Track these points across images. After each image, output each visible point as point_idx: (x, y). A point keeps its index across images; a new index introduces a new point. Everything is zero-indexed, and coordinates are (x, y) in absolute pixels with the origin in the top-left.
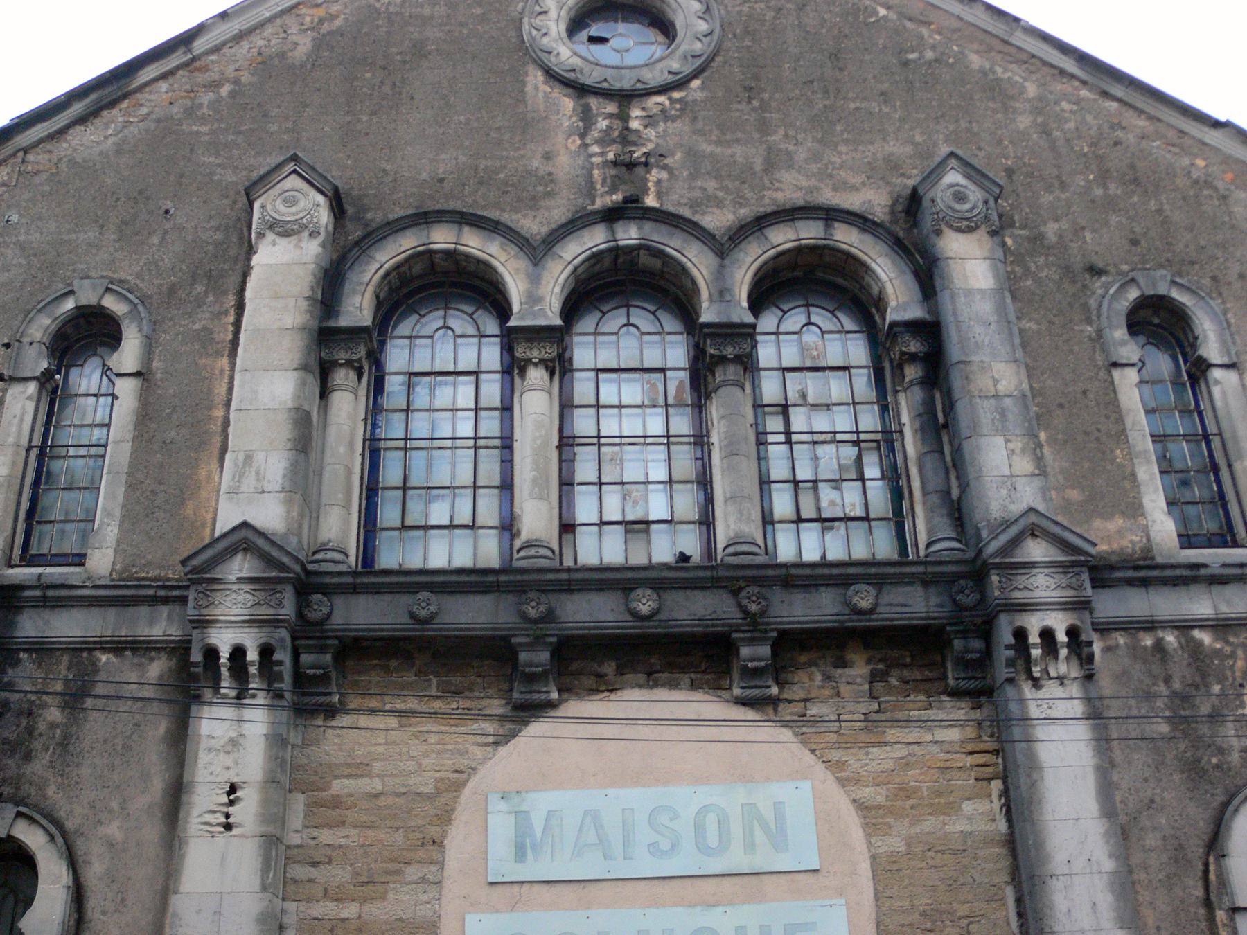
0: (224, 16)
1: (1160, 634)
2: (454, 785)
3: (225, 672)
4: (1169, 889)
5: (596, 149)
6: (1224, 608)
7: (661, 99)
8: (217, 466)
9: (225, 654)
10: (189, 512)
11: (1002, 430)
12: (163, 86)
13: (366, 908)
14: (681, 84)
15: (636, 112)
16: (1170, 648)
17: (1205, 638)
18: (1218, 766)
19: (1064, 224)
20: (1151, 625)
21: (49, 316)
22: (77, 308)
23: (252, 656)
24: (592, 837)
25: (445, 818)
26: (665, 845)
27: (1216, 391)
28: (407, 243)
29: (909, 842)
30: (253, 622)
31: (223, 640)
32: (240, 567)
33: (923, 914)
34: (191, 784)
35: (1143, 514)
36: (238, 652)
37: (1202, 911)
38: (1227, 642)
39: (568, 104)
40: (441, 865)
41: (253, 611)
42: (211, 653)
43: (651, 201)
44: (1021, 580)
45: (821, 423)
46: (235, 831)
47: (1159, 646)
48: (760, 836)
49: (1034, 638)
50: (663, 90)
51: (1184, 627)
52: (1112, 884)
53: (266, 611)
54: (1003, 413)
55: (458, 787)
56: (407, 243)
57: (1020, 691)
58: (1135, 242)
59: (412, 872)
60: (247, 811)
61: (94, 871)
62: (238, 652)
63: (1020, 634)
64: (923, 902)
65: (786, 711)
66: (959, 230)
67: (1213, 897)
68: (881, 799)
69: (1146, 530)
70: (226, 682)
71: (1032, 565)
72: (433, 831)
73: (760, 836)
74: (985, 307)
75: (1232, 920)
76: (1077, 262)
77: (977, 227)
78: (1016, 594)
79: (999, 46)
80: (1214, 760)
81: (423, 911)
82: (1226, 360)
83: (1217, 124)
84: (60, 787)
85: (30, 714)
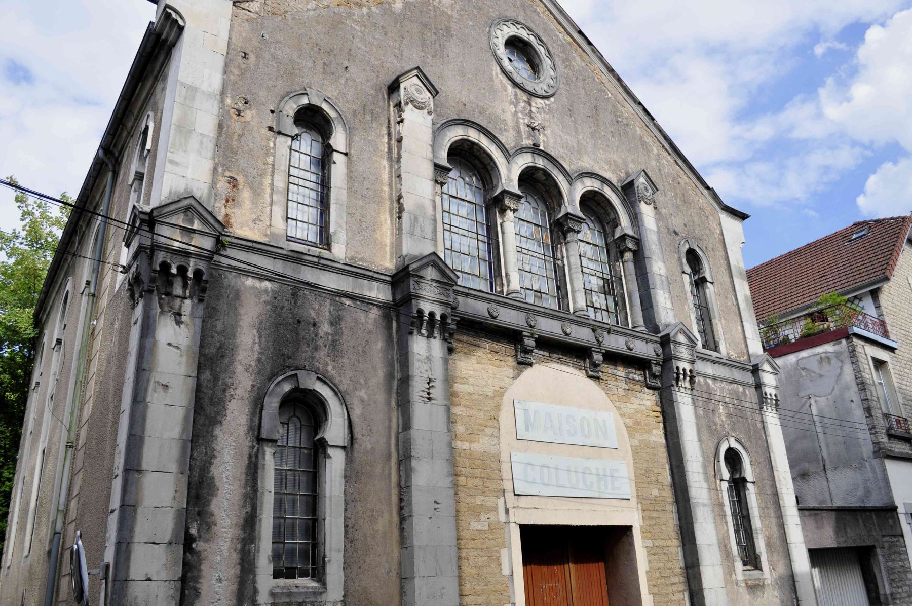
3: (425, 324)
5: (520, 115)
9: (426, 313)
10: (378, 236)
11: (663, 289)
13: (472, 445)
21: (295, 103)
22: (309, 104)
23: (438, 317)
27: (707, 291)
29: (640, 441)
30: (441, 303)
31: (427, 307)
34: (412, 376)
36: (432, 314)
41: (438, 296)
42: (420, 312)
43: (541, 148)
46: (433, 402)
53: (443, 298)
55: (501, 395)
58: (685, 225)
61: (356, 413)
62: (432, 314)
81: (493, 449)
83: (708, 188)
84: (334, 368)
85: (314, 325)
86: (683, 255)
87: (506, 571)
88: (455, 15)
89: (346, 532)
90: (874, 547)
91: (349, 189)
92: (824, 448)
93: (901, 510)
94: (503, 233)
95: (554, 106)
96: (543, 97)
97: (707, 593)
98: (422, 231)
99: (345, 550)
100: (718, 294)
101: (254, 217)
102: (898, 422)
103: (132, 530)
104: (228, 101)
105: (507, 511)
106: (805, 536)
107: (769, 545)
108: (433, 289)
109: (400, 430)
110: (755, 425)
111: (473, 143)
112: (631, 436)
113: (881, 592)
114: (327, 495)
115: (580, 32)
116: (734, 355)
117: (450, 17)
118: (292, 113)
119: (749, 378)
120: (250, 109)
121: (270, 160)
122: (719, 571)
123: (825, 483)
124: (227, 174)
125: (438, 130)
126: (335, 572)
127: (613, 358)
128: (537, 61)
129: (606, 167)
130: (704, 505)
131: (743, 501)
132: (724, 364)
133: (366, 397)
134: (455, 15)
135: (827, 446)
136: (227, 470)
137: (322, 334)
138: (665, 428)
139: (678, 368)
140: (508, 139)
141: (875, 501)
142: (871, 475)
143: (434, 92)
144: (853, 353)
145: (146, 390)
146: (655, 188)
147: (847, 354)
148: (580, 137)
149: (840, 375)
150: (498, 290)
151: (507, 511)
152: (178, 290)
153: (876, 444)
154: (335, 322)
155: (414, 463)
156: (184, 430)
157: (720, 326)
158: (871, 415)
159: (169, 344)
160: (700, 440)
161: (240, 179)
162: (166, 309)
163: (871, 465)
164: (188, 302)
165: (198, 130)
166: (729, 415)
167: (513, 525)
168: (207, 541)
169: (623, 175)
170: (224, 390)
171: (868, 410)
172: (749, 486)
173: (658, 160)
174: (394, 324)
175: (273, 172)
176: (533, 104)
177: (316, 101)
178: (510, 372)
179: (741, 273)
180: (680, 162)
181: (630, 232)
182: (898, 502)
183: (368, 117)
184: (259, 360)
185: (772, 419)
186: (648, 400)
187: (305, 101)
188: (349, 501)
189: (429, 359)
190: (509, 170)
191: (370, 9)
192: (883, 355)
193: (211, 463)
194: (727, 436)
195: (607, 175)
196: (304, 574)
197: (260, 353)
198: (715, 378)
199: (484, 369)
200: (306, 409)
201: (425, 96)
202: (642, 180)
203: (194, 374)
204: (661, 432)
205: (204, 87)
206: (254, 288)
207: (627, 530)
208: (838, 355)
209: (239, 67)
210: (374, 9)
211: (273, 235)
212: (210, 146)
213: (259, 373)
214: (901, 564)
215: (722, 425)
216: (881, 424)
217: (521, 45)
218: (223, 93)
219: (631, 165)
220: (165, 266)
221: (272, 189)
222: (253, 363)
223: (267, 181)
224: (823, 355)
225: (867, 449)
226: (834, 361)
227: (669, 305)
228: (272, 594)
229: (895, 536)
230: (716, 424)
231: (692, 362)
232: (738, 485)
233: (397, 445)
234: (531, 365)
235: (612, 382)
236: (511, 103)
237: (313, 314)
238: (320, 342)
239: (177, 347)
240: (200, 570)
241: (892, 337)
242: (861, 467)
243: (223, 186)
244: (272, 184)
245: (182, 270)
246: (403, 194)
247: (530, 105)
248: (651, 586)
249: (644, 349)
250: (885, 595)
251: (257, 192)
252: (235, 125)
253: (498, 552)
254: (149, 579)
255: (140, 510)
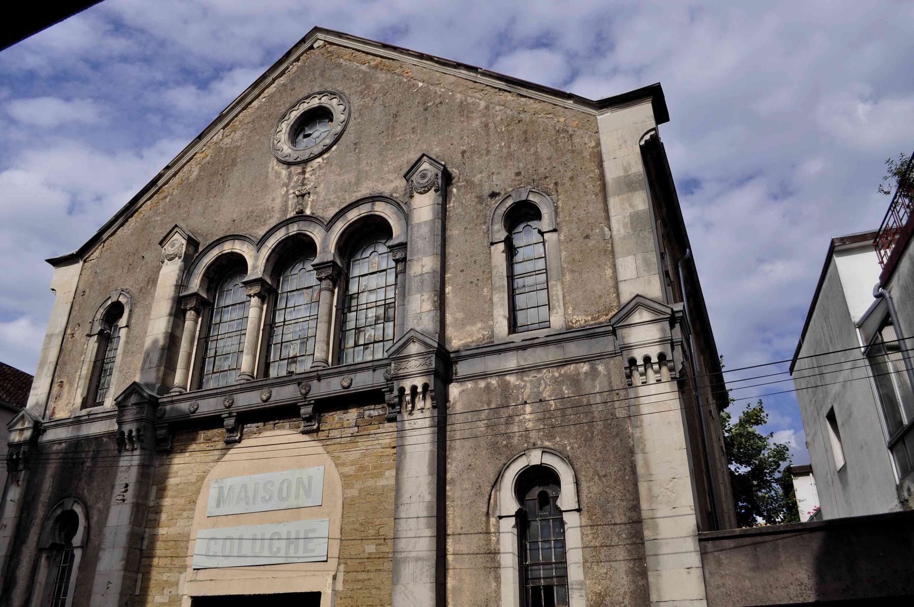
0: (168, 168)
1: (489, 380)
2: (201, 479)
4: (470, 508)
6: (522, 363)
7: (320, 160)
12: (149, 202)
14: (328, 149)
15: (309, 169)
16: (492, 387)
17: (512, 379)
18: (506, 446)
19: (484, 174)
20: (484, 376)
24: (243, 495)
25: (198, 492)
26: (267, 497)
28: (215, 253)
29: (360, 491)
30: (136, 420)
33: (361, 524)
35: (492, 320)
37: (484, 519)
38: (522, 380)
40: (194, 510)
43: (308, 212)
44: (404, 365)
45: (373, 298)
47: (488, 387)
48: (302, 492)
49: (408, 391)
50: (320, 155)
51: (501, 374)
52: (428, 507)
54: (422, 283)
56: (215, 253)
57: (403, 417)
59: (185, 514)
63: (402, 390)
64: (361, 518)
65: (322, 435)
66: (421, 193)
67: (490, 512)
68: (352, 473)
69: (492, 328)
71: (409, 356)
72: (194, 497)
73: (302, 492)
74: (425, 230)
75: (498, 522)
76: (487, 191)
77: (429, 190)
78: (401, 371)
79: (470, 84)
80: (504, 442)
82: (551, 228)
115: (385, 46)
167: (185, 597)
180: (524, 91)
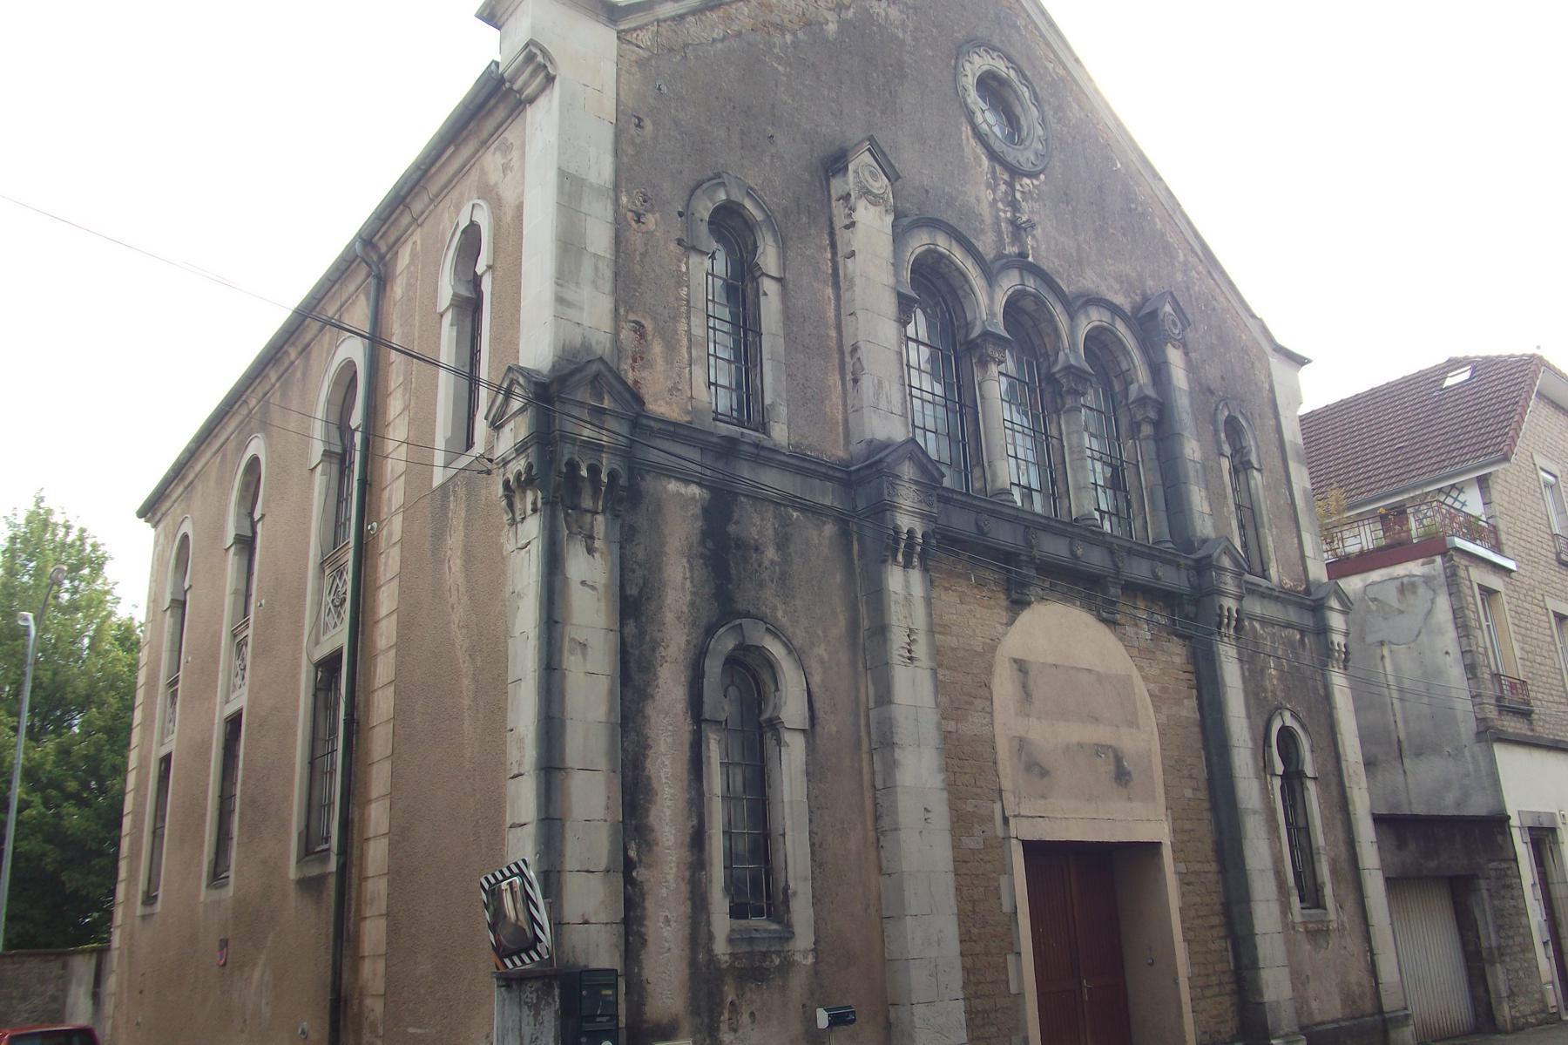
5: (1000, 205)
8: (837, 377)
21: (711, 200)
27: (1252, 483)
32: (907, 471)
36: (910, 532)
39: (985, 161)
42: (897, 531)
55: (993, 649)
60: (921, 650)
61: (816, 679)
62: (910, 532)
70: (900, 558)
83: (1253, 316)
84: (785, 613)
85: (757, 549)
86: (1221, 427)
87: (1007, 908)
88: (909, 40)
89: (813, 853)
90: (1476, 877)
91: (787, 335)
92: (1400, 724)
93: (1514, 821)
94: (982, 397)
95: (1044, 188)
96: (1030, 175)
97: (1259, 940)
98: (889, 402)
99: (813, 879)
100: (1267, 487)
101: (670, 384)
102: (1513, 686)
103: (561, 854)
104: (624, 199)
105: (1006, 820)
106: (1382, 860)
107: (1333, 871)
108: (911, 494)
109: (872, 705)
110: (1316, 690)
111: (941, 255)
112: (1157, 710)
113: (1484, 944)
114: (786, 799)
116: (1288, 584)
117: (903, 43)
118: (706, 216)
119: (1308, 620)
120: (652, 211)
121: (684, 292)
122: (1275, 908)
123: (1401, 778)
124: (632, 317)
125: (899, 235)
126: (802, 913)
127: (1133, 589)
128: (1018, 110)
129: (1117, 287)
130: (1255, 812)
131: (1299, 805)
132: (1276, 599)
133: (826, 657)
134: (909, 40)
135: (1406, 721)
136: (666, 766)
137: (766, 563)
138: (1199, 698)
139: (1221, 607)
140: (986, 244)
141: (1478, 806)
142: (1471, 767)
143: (893, 176)
144: (1452, 580)
145: (561, 651)
146: (1186, 323)
147: (1442, 579)
148: (1081, 238)
149: (1430, 612)
150: (978, 485)
151: (1006, 820)
152: (587, 503)
153: (1480, 721)
154: (783, 543)
155: (898, 754)
156: (611, 710)
157: (1270, 539)
158: (1475, 676)
159: (583, 583)
160: (1249, 716)
161: (649, 325)
162: (575, 529)
163: (1473, 756)
164: (600, 518)
165: (591, 249)
166: (1282, 678)
168: (649, 866)
169: (1138, 299)
170: (654, 649)
171: (1471, 669)
172: (1310, 785)
173: (1185, 273)
174: (856, 547)
175: (689, 312)
176: (1018, 187)
177: (737, 196)
178: (1004, 616)
179: (1298, 454)
181: (1150, 392)
182: (1511, 811)
183: (804, 220)
184: (692, 604)
185: (1338, 680)
186: (1176, 653)
187: (722, 196)
188: (816, 805)
189: (908, 598)
190: (991, 299)
191: (794, 34)
192: (1494, 582)
193: (645, 756)
194: (1279, 708)
195: (1119, 300)
196: (759, 913)
197: (693, 594)
198: (1264, 622)
199: (970, 611)
200: (751, 675)
201: (880, 184)
202: (1168, 308)
203: (617, 627)
204: (1193, 703)
205: (592, 178)
206: (679, 494)
207: (1155, 846)
208: (1428, 580)
209: (633, 143)
210: (800, 35)
211: (695, 412)
212: (607, 273)
213: (694, 624)
214: (1512, 903)
215: (1274, 692)
216: (1490, 691)
217: (995, 84)
218: (616, 187)
219: (1150, 283)
220: (573, 466)
221: (690, 340)
222: (685, 609)
223: (683, 327)
224: (1406, 580)
225: (1468, 728)
226: (1422, 590)
227: (1206, 509)
228: (731, 941)
229: (1505, 860)
230: (1265, 690)
231: (1240, 598)
232: (1293, 780)
233: (868, 726)
234: (1029, 604)
235: (1130, 630)
236: (988, 186)
237: (754, 531)
238: (765, 575)
239: (593, 588)
240: (644, 909)
241: (1507, 550)
242: (1456, 755)
243: (626, 335)
244: (689, 332)
245: (594, 470)
246: (861, 344)
247: (1013, 189)
248: (1185, 930)
249: (1172, 578)
250: (1490, 948)
251: (671, 347)
252: (636, 240)
253: (997, 880)
254: (586, 922)
255: (568, 824)
